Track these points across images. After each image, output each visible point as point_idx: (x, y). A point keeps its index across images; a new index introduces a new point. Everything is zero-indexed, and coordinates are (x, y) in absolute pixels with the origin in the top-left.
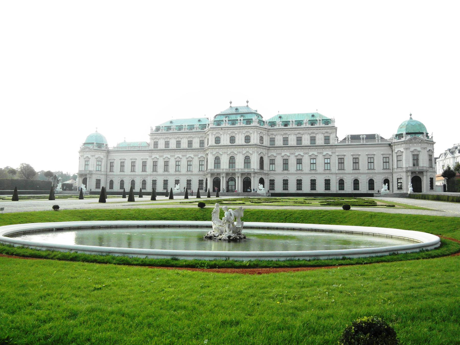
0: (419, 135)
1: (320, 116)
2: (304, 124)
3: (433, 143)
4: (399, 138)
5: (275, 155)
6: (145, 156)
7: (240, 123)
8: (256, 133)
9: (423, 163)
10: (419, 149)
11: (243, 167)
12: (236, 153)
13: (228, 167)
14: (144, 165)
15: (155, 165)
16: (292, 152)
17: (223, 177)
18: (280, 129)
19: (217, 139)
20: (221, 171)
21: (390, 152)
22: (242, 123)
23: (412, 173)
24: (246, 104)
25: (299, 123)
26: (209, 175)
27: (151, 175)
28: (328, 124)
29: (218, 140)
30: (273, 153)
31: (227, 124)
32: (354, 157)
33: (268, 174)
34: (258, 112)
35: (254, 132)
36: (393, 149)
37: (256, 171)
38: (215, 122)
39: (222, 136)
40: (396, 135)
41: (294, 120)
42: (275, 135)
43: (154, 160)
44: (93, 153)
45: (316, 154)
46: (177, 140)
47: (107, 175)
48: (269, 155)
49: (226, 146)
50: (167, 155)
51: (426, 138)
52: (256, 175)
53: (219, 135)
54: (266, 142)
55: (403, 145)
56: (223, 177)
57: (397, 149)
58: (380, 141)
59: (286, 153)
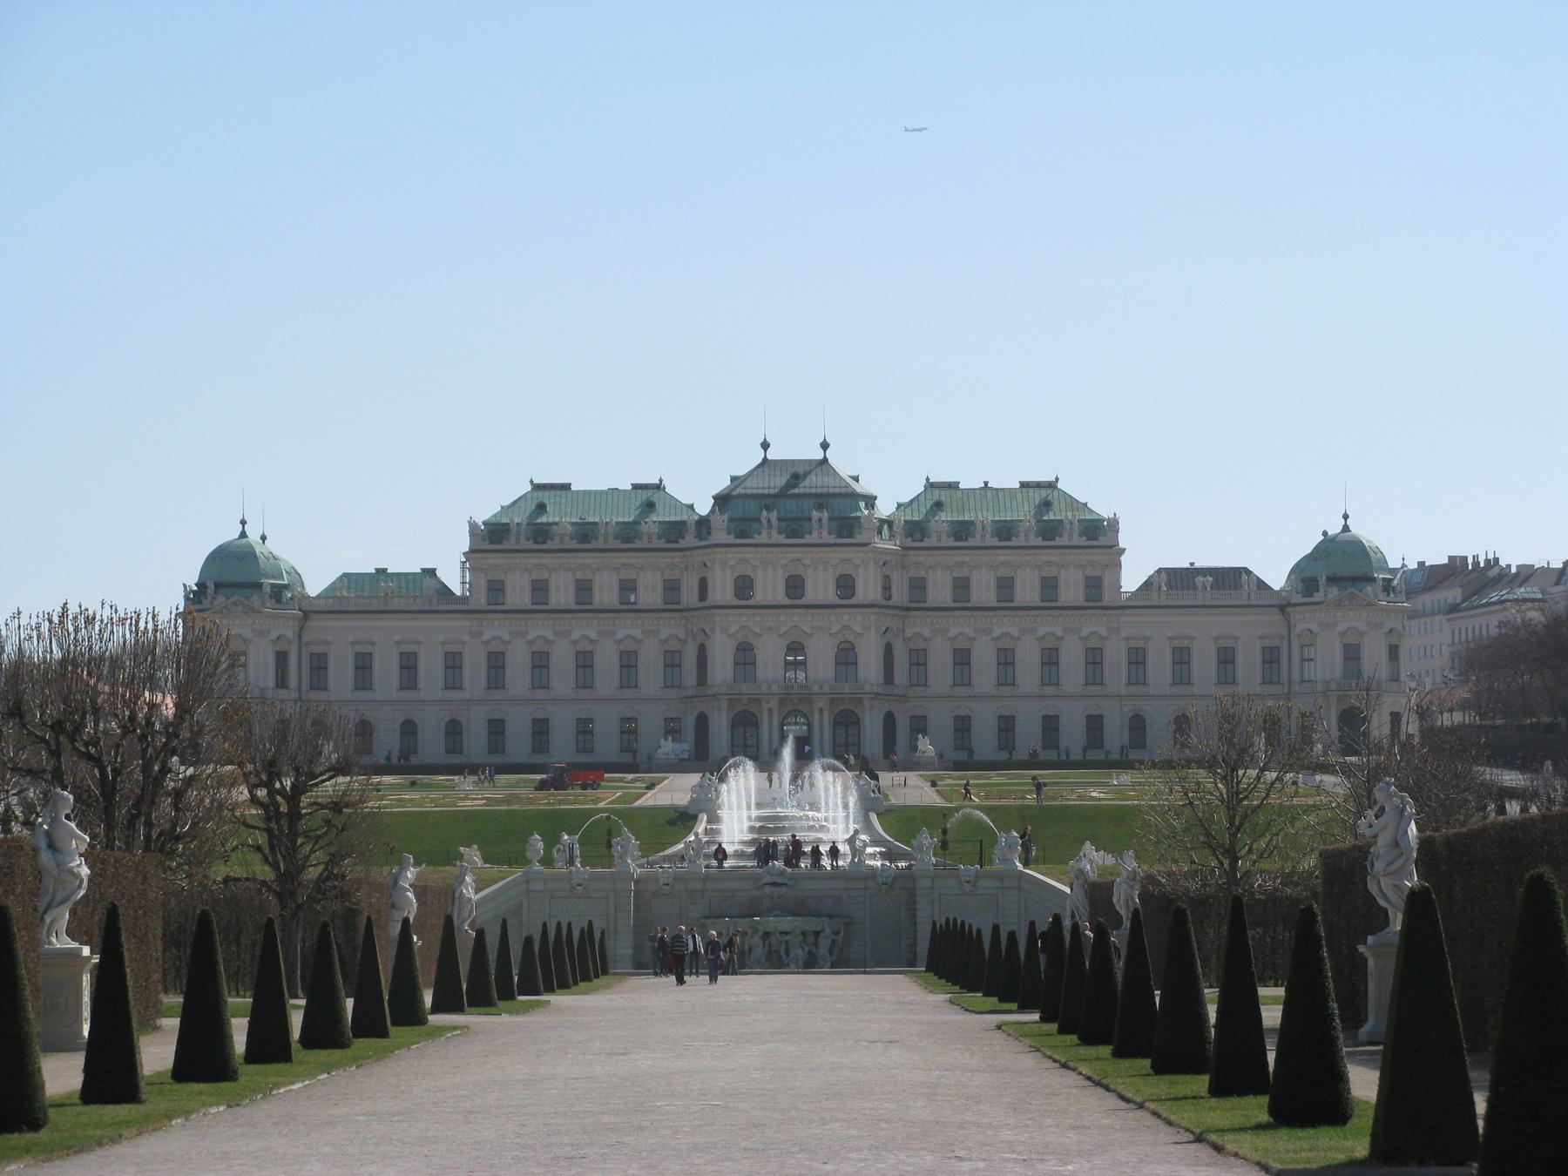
1: (1072, 503)
2: (1022, 536)
5: (926, 632)
8: (871, 567)
10: (1361, 626)
11: (831, 674)
12: (807, 629)
14: (453, 663)
15: (496, 663)
17: (770, 711)
20: (764, 689)
21: (1284, 632)
25: (1005, 531)
26: (724, 704)
28: (1096, 539)
29: (744, 587)
30: (920, 626)
31: (774, 533)
32: (1177, 643)
33: (904, 698)
34: (864, 487)
37: (876, 689)
39: (759, 572)
43: (490, 649)
45: (1060, 634)
46: (579, 575)
48: (908, 633)
53: (748, 571)
54: (900, 595)
56: (770, 711)
59: (961, 627)
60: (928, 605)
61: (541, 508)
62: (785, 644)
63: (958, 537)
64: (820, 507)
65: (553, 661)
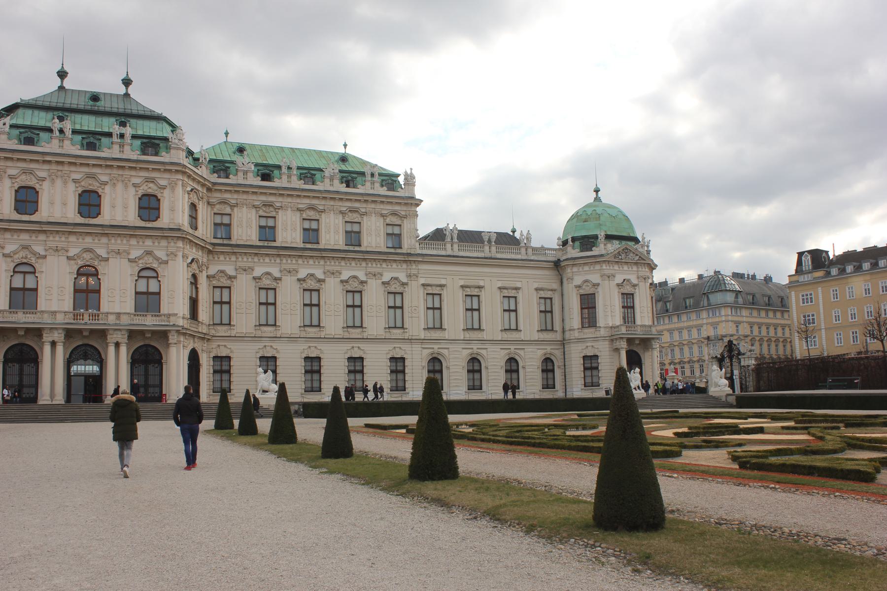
0: (631, 244)
1: (364, 163)
2: (327, 181)
4: (582, 245)
5: (230, 271)
7: (122, 146)
8: (179, 189)
9: (644, 315)
11: (129, 306)
12: (102, 252)
13: (67, 304)
16: (288, 267)
17: (53, 344)
18: (251, 186)
19: (22, 197)
20: (47, 319)
21: (555, 286)
22: (127, 148)
23: (630, 341)
24: (122, 90)
25: (309, 174)
32: (469, 291)
33: (205, 338)
35: (173, 186)
37: (181, 322)
38: (16, 132)
39: (46, 185)
40: (574, 239)
41: (294, 165)
42: (233, 207)
45: (363, 278)
48: (213, 270)
49: (65, 224)
52: (182, 339)
53: (32, 182)
54: (205, 230)
55: (598, 267)
56: (53, 344)
57: (578, 277)
58: (530, 251)
60: (233, 242)
62: (76, 268)
63: (266, 177)
64: (123, 124)
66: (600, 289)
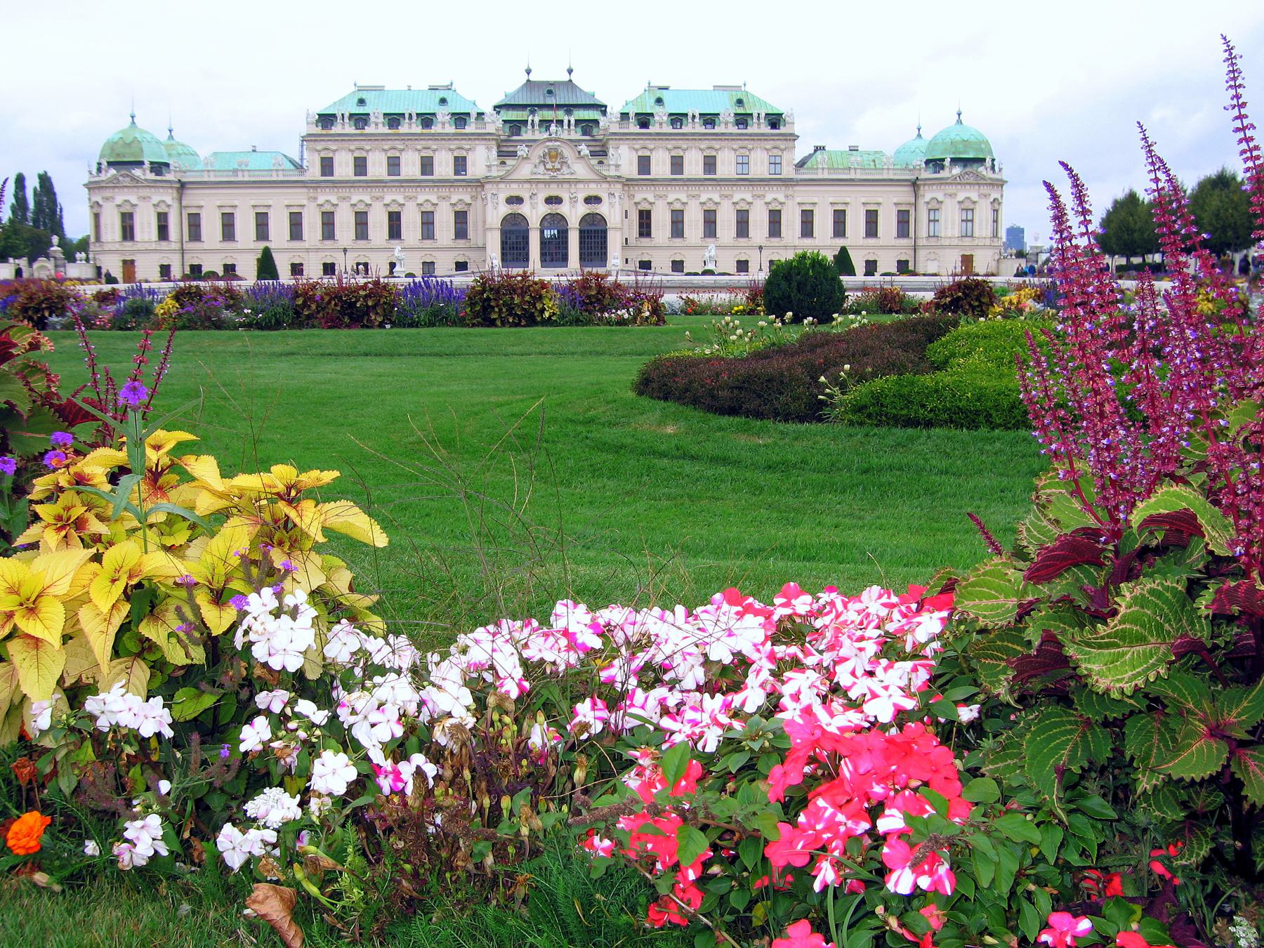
0: (975, 166)
3: (1000, 184)
5: (651, 199)
6: (298, 198)
10: (974, 196)
25: (709, 119)
27: (318, 250)
36: (921, 192)
40: (928, 162)
43: (324, 209)
44: (145, 192)
45: (750, 200)
47: (183, 251)
50: (360, 197)
51: (990, 174)
57: (928, 194)
59: (677, 195)
61: (362, 102)
65: (371, 220)
66: (943, 206)
